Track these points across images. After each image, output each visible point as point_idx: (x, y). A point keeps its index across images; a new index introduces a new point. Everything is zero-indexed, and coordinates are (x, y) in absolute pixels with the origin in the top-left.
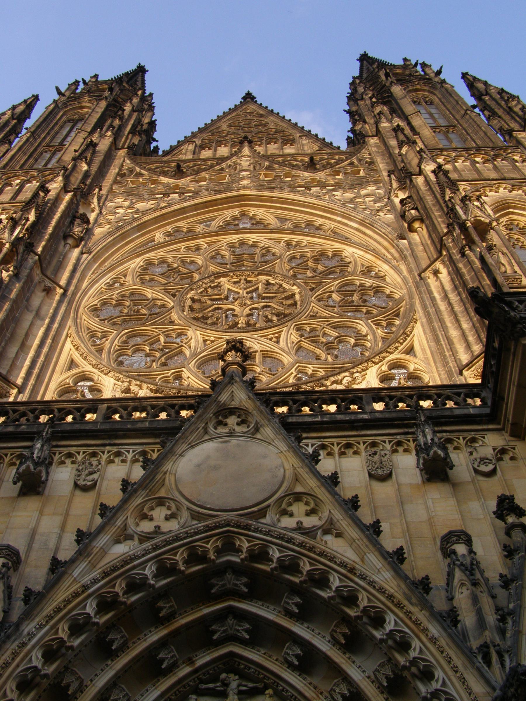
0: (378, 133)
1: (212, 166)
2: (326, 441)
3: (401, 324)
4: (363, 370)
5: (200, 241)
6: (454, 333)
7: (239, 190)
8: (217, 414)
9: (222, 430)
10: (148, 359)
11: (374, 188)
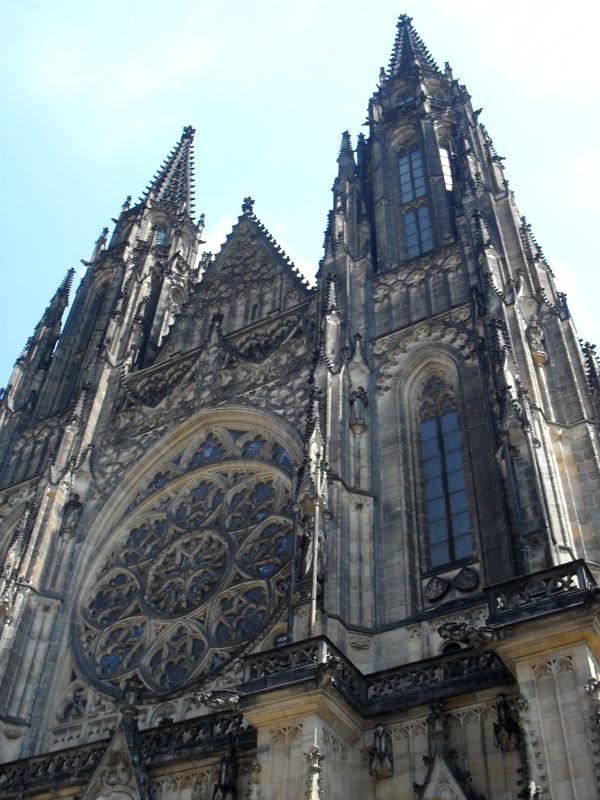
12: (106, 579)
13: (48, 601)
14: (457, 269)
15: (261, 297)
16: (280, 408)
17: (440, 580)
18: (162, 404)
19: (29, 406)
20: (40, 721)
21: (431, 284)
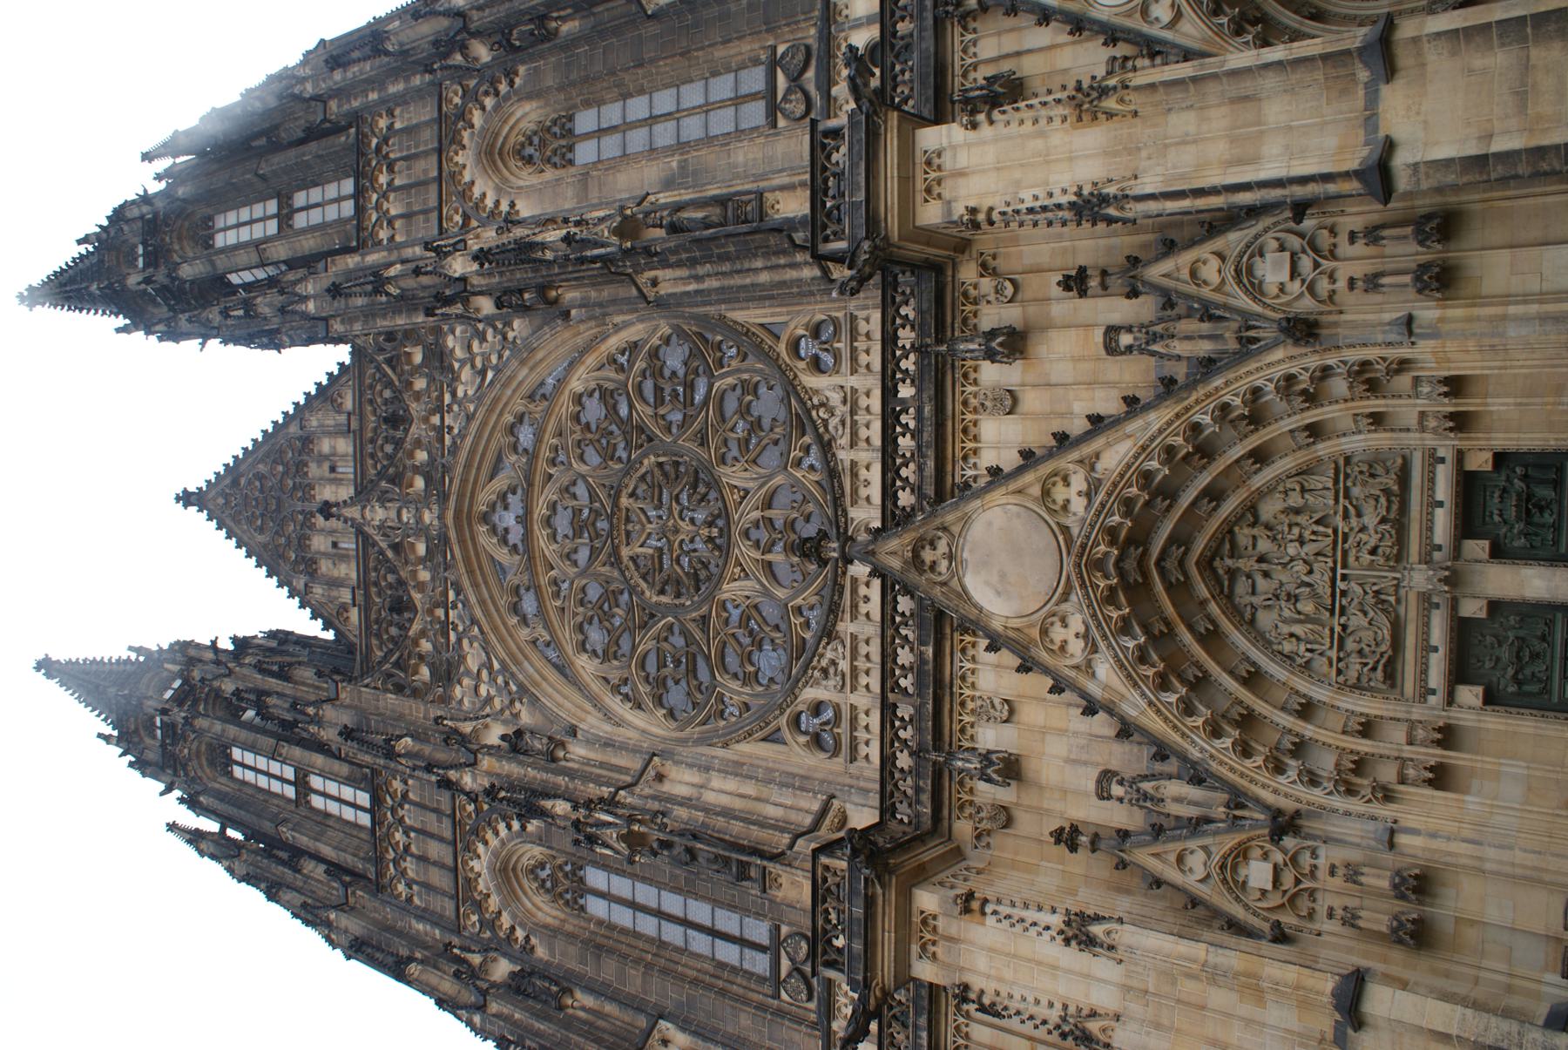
0: (326, 319)
1: (388, 561)
2: (959, 454)
5: (544, 580)
6: (764, 277)
7: (446, 526)
8: (921, 572)
9: (943, 565)
10: (767, 647)
12: (643, 689)
13: (651, 773)
15: (322, 458)
16: (483, 380)
17: (784, 98)
18: (417, 596)
19: (348, 879)
20: (830, 783)
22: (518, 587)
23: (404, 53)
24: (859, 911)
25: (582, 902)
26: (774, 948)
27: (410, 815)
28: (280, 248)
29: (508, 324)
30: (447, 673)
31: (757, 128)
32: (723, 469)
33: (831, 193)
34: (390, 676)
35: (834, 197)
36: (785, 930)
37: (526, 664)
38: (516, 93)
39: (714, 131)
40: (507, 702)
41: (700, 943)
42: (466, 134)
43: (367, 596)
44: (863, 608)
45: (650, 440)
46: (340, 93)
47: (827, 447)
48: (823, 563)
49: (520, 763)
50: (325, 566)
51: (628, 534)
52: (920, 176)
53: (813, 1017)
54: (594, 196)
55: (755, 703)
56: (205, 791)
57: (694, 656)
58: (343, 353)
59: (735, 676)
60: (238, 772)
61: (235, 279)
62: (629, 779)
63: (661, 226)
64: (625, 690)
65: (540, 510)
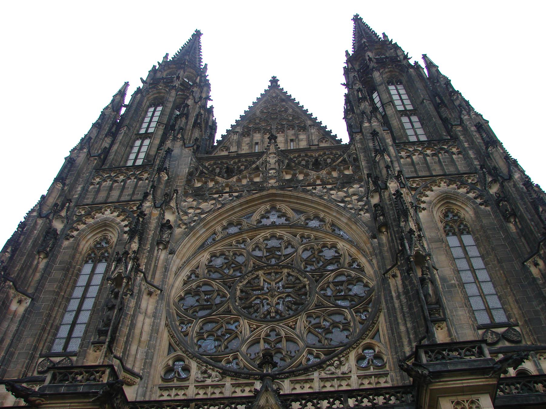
0: (361, 132)
1: (251, 165)
3: (371, 311)
4: (347, 354)
5: (245, 236)
6: (402, 328)
7: (268, 190)
10: (217, 343)
11: (358, 186)
12: (194, 285)
13: (152, 289)
14: (458, 154)
15: (297, 136)
18: (234, 179)
19: (102, 157)
20: (149, 377)
21: (441, 158)
22: (241, 225)
23: (488, 156)
24: (81, 389)
25: (90, 262)
26: (65, 354)
27: (131, 182)
28: (391, 111)
29: (367, 211)
30: (199, 194)
31: (476, 320)
32: (304, 316)
33: (450, 353)
34: (197, 169)
35: (448, 355)
36: (74, 358)
37: (204, 230)
38: (477, 207)
39: (472, 300)
40: (185, 222)
41: (69, 318)
42: (454, 186)
43: (234, 158)
44: (238, 390)
45: (317, 281)
46: (465, 130)
47: (320, 366)
48: (260, 366)
49: (156, 228)
50: (247, 140)
51: (270, 274)
52: (465, 398)
53: (30, 374)
54: (433, 245)
55: (188, 339)
56: (143, 96)
57: (211, 308)
58: (345, 139)
59: (201, 328)
60: (152, 109)
61: (375, 95)
62: (149, 279)
63: (423, 274)
64: (193, 277)
65: (278, 232)
